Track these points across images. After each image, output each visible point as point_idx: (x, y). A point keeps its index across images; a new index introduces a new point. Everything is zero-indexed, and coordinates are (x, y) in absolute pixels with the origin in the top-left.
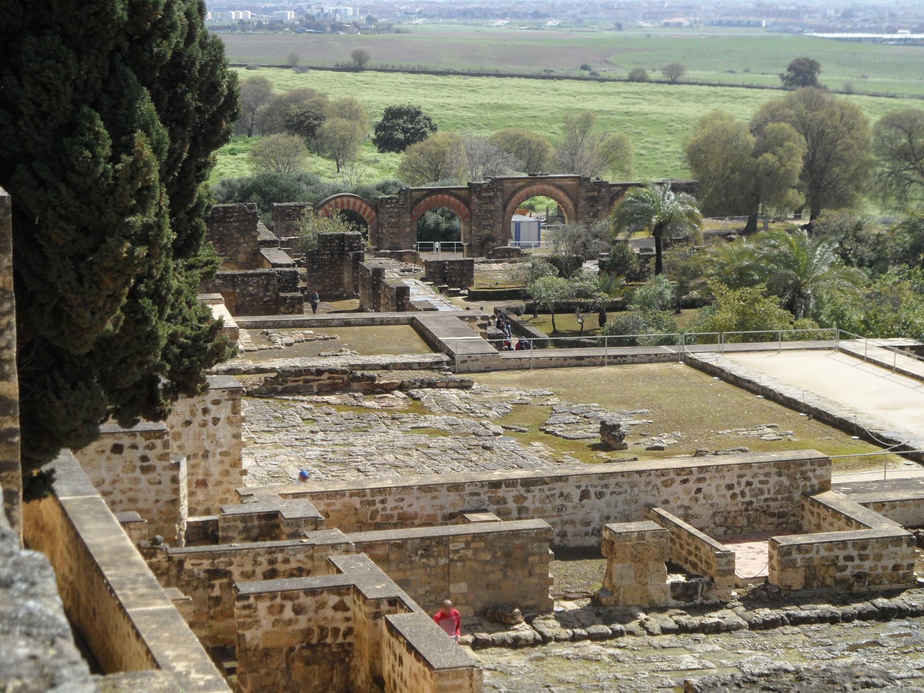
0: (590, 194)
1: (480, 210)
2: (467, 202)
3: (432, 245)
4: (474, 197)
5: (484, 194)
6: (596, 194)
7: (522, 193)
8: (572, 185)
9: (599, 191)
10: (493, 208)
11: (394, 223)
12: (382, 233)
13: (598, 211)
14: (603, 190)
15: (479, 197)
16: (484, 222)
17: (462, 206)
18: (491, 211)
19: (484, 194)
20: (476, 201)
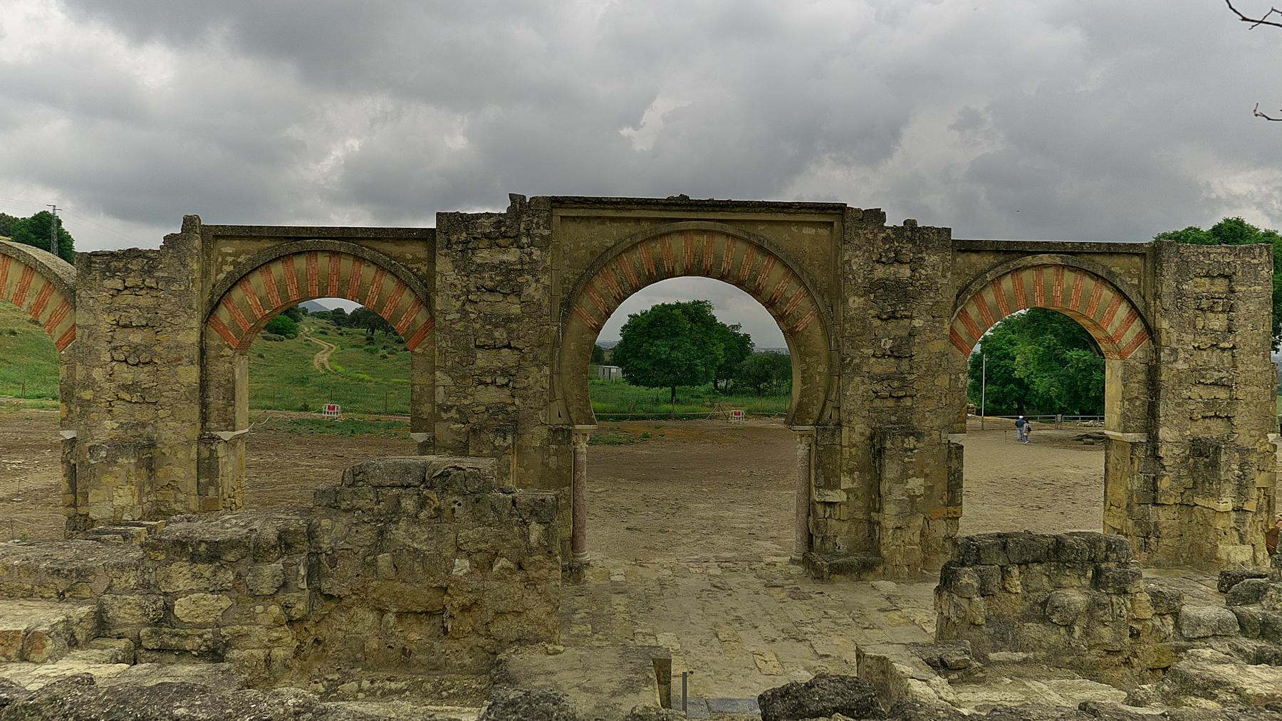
0: (880, 272)
1: (464, 314)
4: (444, 265)
5: (484, 255)
6: (905, 272)
9: (915, 264)
10: (516, 309)
11: (135, 349)
12: (89, 383)
14: (932, 259)
15: (464, 267)
16: (482, 359)
18: (508, 319)
20: (452, 276)
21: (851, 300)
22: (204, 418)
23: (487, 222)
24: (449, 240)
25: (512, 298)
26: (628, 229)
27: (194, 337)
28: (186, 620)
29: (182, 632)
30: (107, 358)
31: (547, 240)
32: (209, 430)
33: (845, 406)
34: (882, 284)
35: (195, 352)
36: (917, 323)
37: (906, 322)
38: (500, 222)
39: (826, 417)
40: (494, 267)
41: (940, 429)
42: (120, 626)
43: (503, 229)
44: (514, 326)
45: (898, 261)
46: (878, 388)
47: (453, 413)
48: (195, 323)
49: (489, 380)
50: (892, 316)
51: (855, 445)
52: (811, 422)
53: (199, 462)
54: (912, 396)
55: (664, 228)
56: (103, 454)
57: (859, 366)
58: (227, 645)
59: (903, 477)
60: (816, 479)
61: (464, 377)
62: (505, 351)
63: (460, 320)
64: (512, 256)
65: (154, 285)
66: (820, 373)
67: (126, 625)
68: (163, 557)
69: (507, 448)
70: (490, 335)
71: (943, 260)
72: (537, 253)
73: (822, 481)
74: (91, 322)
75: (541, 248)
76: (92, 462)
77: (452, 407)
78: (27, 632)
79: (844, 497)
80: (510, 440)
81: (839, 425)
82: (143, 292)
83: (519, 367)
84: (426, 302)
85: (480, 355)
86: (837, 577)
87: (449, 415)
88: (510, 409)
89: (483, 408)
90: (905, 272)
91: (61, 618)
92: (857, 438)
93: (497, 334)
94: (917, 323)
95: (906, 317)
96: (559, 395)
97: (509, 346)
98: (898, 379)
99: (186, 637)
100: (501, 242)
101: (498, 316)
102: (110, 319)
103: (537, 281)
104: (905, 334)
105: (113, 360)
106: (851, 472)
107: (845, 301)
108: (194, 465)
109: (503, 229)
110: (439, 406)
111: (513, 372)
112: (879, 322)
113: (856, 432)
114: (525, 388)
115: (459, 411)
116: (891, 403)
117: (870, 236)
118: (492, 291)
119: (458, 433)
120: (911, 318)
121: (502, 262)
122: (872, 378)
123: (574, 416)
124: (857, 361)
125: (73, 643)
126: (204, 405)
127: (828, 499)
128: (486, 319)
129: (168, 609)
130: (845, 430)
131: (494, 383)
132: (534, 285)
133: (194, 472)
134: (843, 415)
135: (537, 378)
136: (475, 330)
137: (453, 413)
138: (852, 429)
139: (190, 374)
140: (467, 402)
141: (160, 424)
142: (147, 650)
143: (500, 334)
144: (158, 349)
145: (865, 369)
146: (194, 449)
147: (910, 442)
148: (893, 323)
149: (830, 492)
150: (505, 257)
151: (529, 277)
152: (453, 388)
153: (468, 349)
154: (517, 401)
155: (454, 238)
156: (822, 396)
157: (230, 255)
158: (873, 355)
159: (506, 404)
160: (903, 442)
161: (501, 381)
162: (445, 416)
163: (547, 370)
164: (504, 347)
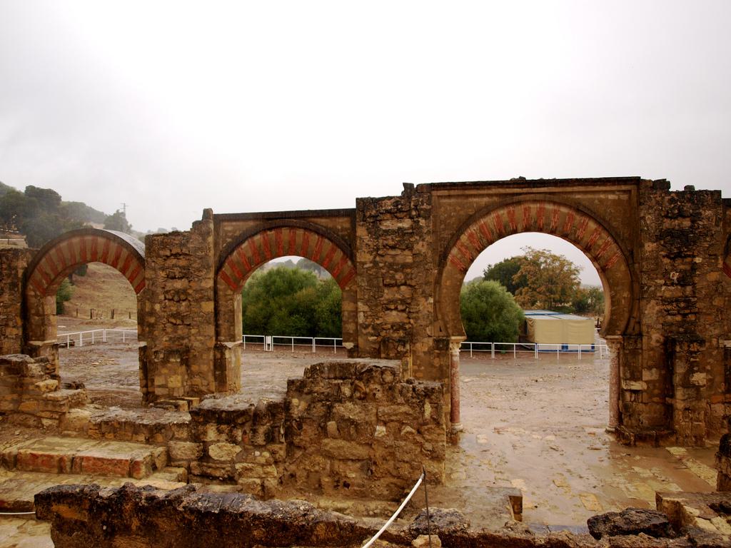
0: (667, 224)
1: (375, 263)
2: (348, 246)
3: (261, 340)
4: (361, 232)
5: (388, 224)
6: (687, 223)
7: (490, 220)
8: (617, 203)
9: (695, 218)
10: (409, 260)
11: (177, 292)
12: (152, 313)
13: (694, 267)
15: (375, 232)
16: (388, 294)
17: (339, 255)
18: (405, 266)
19: (388, 224)
20: (367, 238)
21: (646, 245)
22: (217, 334)
23: (389, 203)
24: (364, 216)
25: (407, 252)
26: (486, 200)
27: (211, 283)
28: (216, 458)
29: (214, 465)
30: (162, 297)
31: (428, 212)
32: (220, 341)
33: (646, 321)
34: (670, 232)
35: (211, 294)
36: (698, 260)
37: (688, 260)
38: (397, 201)
39: (630, 330)
40: (394, 232)
41: (718, 337)
42: (179, 460)
43: (400, 207)
44: (409, 270)
45: (681, 215)
46: (669, 307)
47: (370, 330)
48: (212, 275)
49: (393, 307)
50: (679, 255)
51: (652, 349)
52: (619, 333)
53: (215, 360)
54: (695, 313)
55: (508, 200)
56: (162, 356)
57: (654, 292)
58: (240, 475)
59: (690, 371)
60: (624, 374)
61: (376, 306)
62: (403, 288)
63: (373, 267)
64: (406, 224)
65: (187, 252)
66: (624, 298)
67: (183, 460)
68: (202, 420)
69: (406, 352)
70: (393, 277)
71: (716, 214)
72: (422, 222)
73: (628, 375)
74: (153, 276)
75: (425, 218)
76: (156, 360)
77: (369, 325)
78: (132, 461)
79: (645, 387)
80: (408, 347)
81: (640, 335)
82: (181, 257)
83: (412, 298)
84: (350, 254)
85: (386, 291)
86: (641, 444)
87: (367, 331)
88: (407, 326)
89: (389, 326)
90: (687, 223)
91: (149, 454)
92: (653, 343)
93: (397, 277)
94: (698, 260)
95: (689, 256)
96: (440, 316)
97: (405, 284)
98: (684, 301)
99: (217, 468)
100: (398, 215)
101: (398, 264)
102: (163, 274)
103: (423, 240)
104: (688, 267)
105: (165, 299)
106: (650, 368)
107: (642, 246)
108: (212, 363)
109: (400, 207)
110: (361, 325)
111: (409, 301)
112: (668, 261)
113: (655, 337)
114: (417, 312)
115: (373, 328)
116: (679, 318)
117: (658, 199)
118: (393, 248)
119: (374, 342)
120: (694, 257)
121: (400, 228)
122: (665, 301)
123: (450, 331)
124: (652, 289)
125: (154, 468)
126: (217, 326)
127: (633, 388)
128: (391, 266)
129: (205, 451)
130: (645, 339)
131: (396, 309)
132: (421, 243)
133: (212, 367)
134: (644, 329)
135: (425, 305)
136: (383, 274)
137: (370, 330)
138: (650, 338)
139: (209, 307)
140: (378, 322)
141: (192, 338)
142: (194, 475)
143: (399, 276)
144: (190, 291)
145: (659, 294)
146: (212, 354)
147: (695, 347)
148: (678, 261)
149: (634, 383)
150: (400, 225)
151: (418, 238)
152: (369, 313)
153: (379, 287)
154: (412, 321)
155: (368, 214)
156: (626, 315)
157: (230, 232)
158: (665, 284)
159: (404, 324)
160: (689, 346)
161: (400, 307)
162: (364, 331)
163: (431, 300)
164: (402, 285)
